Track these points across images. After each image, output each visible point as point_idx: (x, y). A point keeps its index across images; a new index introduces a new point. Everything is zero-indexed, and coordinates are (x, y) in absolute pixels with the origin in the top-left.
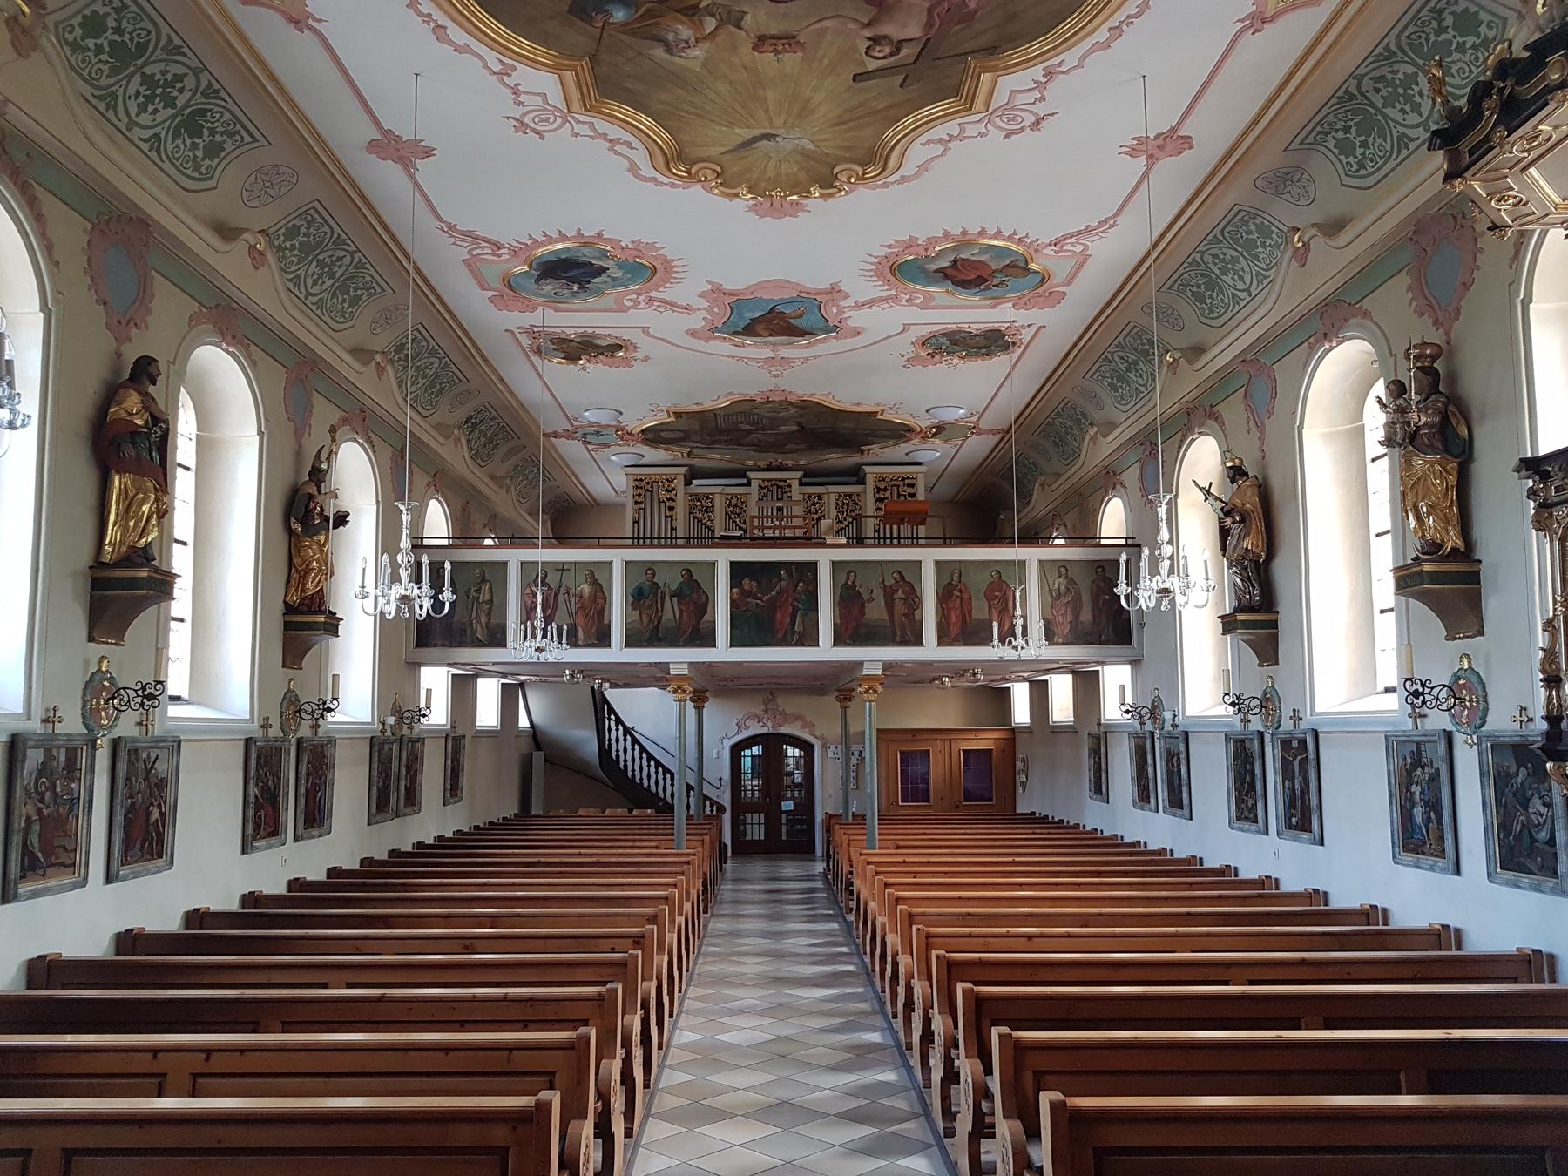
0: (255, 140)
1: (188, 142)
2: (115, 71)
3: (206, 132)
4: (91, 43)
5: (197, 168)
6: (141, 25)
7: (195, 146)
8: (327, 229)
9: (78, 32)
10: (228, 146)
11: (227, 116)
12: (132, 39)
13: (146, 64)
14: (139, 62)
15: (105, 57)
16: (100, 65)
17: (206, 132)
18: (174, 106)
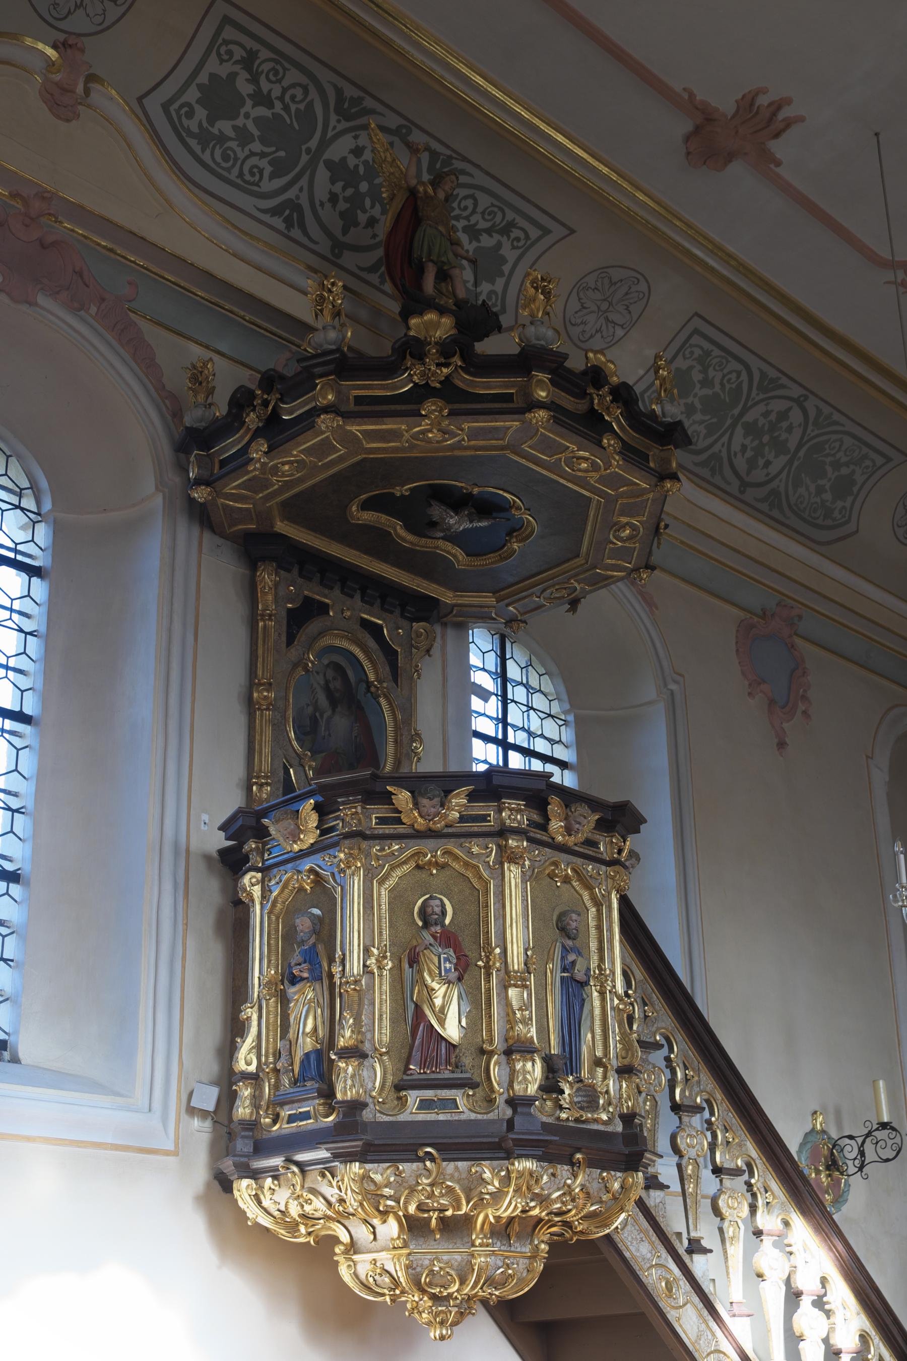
0: (546, 231)
2: (279, 169)
4: (225, 126)
8: (734, 365)
9: (201, 113)
10: (507, 251)
11: (484, 201)
12: (286, 108)
13: (324, 144)
14: (313, 144)
15: (257, 147)
16: (254, 160)
18: (329, 164)
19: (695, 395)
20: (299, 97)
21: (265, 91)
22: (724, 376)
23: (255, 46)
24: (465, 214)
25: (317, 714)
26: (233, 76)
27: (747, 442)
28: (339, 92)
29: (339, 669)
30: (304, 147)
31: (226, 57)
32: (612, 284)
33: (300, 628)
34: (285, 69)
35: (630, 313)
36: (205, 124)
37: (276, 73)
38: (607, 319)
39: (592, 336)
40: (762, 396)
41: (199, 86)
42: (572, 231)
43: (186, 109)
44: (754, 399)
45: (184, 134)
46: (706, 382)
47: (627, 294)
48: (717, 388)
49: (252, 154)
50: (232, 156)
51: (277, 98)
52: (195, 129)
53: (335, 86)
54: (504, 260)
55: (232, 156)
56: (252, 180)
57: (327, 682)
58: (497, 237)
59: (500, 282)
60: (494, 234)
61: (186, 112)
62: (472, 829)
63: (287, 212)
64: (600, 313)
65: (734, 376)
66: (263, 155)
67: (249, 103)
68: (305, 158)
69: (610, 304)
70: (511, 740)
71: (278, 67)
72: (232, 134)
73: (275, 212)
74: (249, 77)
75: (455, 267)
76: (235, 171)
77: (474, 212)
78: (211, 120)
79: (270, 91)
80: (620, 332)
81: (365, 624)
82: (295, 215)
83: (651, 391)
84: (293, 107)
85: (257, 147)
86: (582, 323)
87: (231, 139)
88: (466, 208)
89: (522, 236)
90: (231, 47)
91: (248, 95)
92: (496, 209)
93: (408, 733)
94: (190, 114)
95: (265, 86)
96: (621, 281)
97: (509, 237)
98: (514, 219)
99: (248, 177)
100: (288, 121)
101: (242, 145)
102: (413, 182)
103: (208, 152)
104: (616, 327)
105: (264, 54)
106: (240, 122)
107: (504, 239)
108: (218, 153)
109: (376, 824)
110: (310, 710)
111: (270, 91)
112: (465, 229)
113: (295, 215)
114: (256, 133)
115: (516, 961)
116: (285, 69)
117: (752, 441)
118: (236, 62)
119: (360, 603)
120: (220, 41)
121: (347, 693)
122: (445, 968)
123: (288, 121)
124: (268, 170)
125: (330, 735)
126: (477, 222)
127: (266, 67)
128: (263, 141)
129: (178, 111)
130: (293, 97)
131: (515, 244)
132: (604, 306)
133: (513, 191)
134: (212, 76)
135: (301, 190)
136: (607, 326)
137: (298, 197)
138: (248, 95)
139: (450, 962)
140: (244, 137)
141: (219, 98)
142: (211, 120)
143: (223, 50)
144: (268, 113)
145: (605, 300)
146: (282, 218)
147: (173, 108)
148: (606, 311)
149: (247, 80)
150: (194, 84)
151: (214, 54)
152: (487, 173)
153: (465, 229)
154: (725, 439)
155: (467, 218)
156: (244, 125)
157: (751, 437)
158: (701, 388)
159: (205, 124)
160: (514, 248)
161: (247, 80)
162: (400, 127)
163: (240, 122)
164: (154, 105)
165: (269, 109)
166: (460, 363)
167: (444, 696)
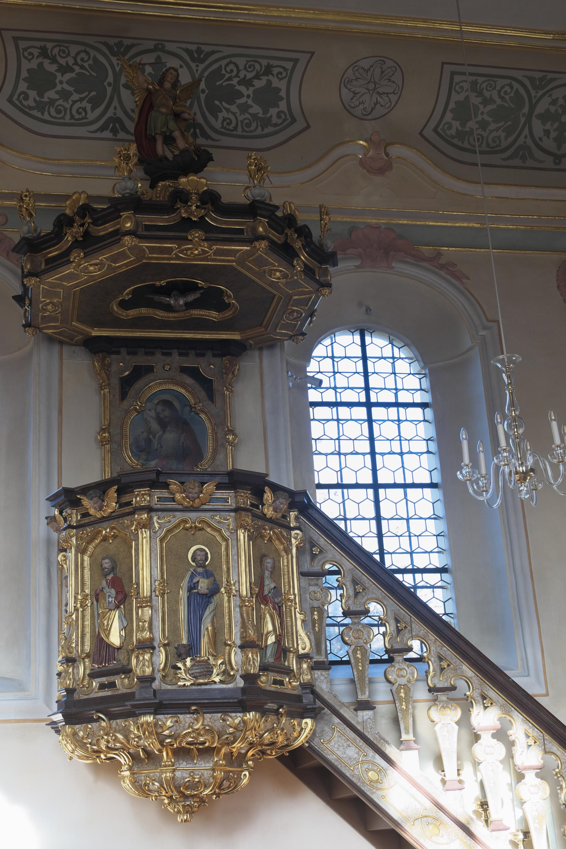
0: (296, 61)
1: (234, 108)
2: (95, 103)
3: (242, 89)
4: (51, 94)
5: (266, 122)
6: (73, 54)
7: (244, 108)
8: (501, 82)
9: (33, 94)
10: (276, 83)
11: (241, 62)
12: (82, 67)
14: (110, 79)
15: (75, 97)
16: (78, 105)
17: (242, 89)
19: (482, 113)
21: (64, 64)
22: (499, 92)
23: (42, 44)
24: (234, 74)
25: (151, 437)
26: (41, 65)
27: (548, 126)
28: (106, 44)
29: (167, 404)
30: (106, 84)
31: (30, 57)
33: (131, 386)
34: (67, 47)
35: (394, 82)
36: (38, 99)
37: (64, 52)
38: (378, 93)
39: (373, 109)
40: (541, 93)
41: (25, 80)
42: (313, 53)
43: (23, 95)
44: (535, 96)
45: (27, 110)
46: (486, 102)
47: (382, 72)
48: (499, 101)
49: (74, 102)
50: (62, 109)
51: (73, 64)
52: (32, 104)
53: (101, 43)
54: (279, 90)
55: (62, 109)
56: (81, 116)
57: (158, 414)
58: (264, 78)
59: (283, 105)
60: (261, 77)
61: (23, 98)
62: (125, 511)
63: (111, 125)
64: (371, 92)
65: (507, 88)
66: (81, 100)
67: (59, 75)
68: (109, 90)
69: (375, 83)
70: (373, 399)
71: (62, 48)
72: (57, 97)
73: (102, 129)
74: (49, 61)
75: (173, 131)
76: (68, 116)
77: (239, 71)
78: (41, 95)
79: (67, 63)
80: (394, 98)
81: (184, 370)
82: (117, 125)
83: (442, 124)
84: (86, 65)
85: (75, 97)
86: (360, 104)
87: (57, 100)
88: (232, 71)
89: (281, 70)
90: (29, 51)
91: (56, 71)
92: (252, 63)
93: (225, 429)
94: (26, 97)
95: (63, 62)
96: (372, 66)
98: (268, 63)
99: (77, 116)
100: (88, 74)
101: (66, 100)
102: (145, 85)
103: (46, 113)
104: (389, 95)
105: (49, 45)
106: (59, 87)
107: (270, 77)
108: (53, 111)
109: (81, 518)
110: (145, 434)
111: (67, 63)
112: (239, 83)
113: (117, 125)
114: (71, 89)
115: (146, 589)
117: (552, 125)
118: (38, 57)
119: (178, 358)
120: (21, 51)
121: (176, 417)
122: (109, 601)
123: (88, 74)
124: (89, 107)
125: (161, 447)
126: (245, 75)
127: (56, 51)
128: (77, 91)
129: (18, 99)
130: (82, 59)
131: (280, 76)
132: (371, 86)
133: (253, 48)
134: (29, 71)
135: (115, 108)
136: (381, 98)
137: (115, 114)
138: (56, 71)
139: (112, 598)
140: (65, 95)
141: (40, 81)
142: (41, 95)
143: (26, 54)
144: (73, 75)
145: (369, 82)
146: (109, 131)
147: (14, 99)
148: (375, 89)
149: (50, 63)
150: (21, 79)
151: (23, 60)
152: (229, 46)
153: (239, 83)
154: (526, 131)
155: (237, 76)
156: (62, 88)
157: (550, 122)
158: (484, 107)
159: (38, 99)
160: (280, 79)
161: (50, 63)
162: (155, 46)
163: (59, 87)
165: (73, 72)
166: (89, 221)
167: (263, 396)
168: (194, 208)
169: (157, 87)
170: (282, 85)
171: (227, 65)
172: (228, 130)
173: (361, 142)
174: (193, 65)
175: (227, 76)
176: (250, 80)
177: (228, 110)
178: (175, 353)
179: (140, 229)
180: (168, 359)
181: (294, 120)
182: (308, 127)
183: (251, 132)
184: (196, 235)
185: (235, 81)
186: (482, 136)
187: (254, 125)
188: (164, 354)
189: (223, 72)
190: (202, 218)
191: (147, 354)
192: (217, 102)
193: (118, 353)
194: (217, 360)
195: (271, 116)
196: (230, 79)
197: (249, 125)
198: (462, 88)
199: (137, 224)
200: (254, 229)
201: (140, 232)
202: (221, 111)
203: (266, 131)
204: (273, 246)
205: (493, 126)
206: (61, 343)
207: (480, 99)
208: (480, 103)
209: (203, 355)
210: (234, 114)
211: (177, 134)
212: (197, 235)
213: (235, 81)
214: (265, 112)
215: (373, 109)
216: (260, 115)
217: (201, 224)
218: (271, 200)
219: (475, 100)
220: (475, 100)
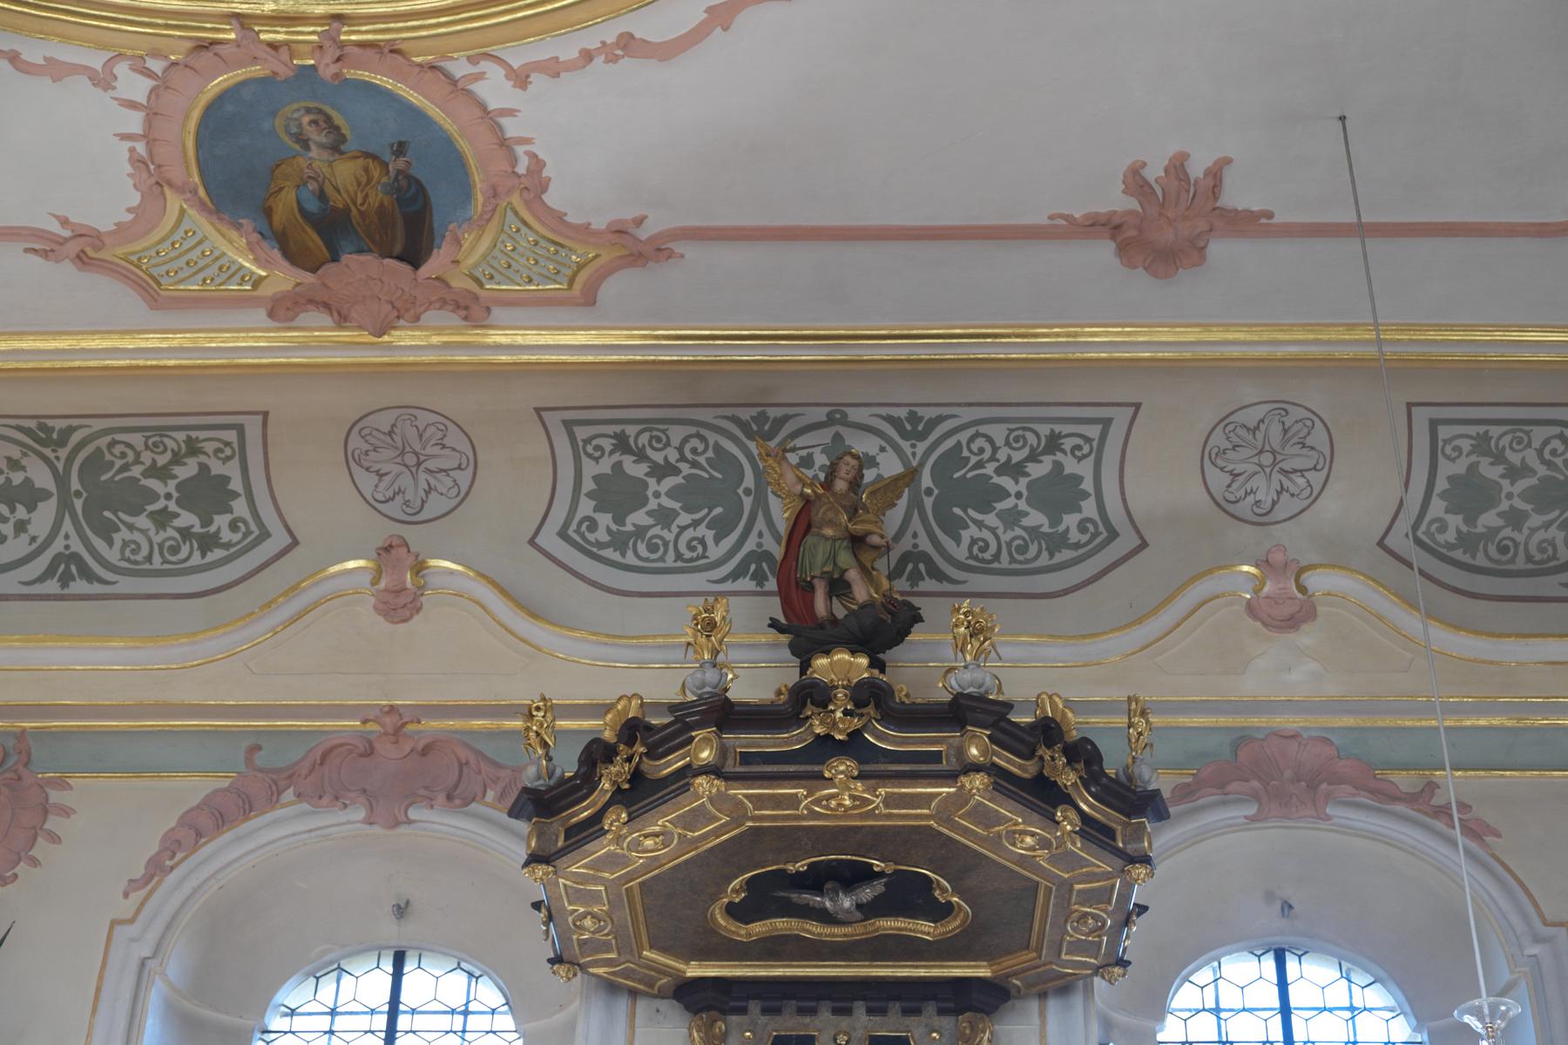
2: (722, 528)
4: (639, 518)
5: (1058, 541)
6: (676, 442)
8: (1539, 434)
9: (605, 520)
10: (1071, 466)
11: (998, 433)
12: (694, 464)
16: (689, 533)
17: (1006, 482)
20: (701, 448)
22: (1540, 452)
23: (618, 428)
26: (618, 466)
28: (735, 420)
30: (740, 491)
31: (598, 454)
32: (1254, 431)
34: (663, 431)
36: (614, 527)
37: (659, 440)
38: (1284, 472)
39: (1274, 503)
41: (590, 495)
42: (1138, 406)
46: (1514, 473)
47: (1285, 431)
48: (1542, 471)
49: (683, 529)
52: (605, 538)
54: (1078, 479)
59: (1089, 508)
63: (753, 567)
64: (1268, 470)
66: (695, 524)
67: (652, 481)
68: (748, 502)
69: (1273, 452)
72: (651, 521)
73: (735, 575)
76: (671, 554)
77: (995, 449)
78: (619, 520)
79: (666, 458)
84: (702, 460)
85: (684, 519)
88: (982, 450)
90: (595, 442)
92: (1020, 432)
94: (593, 526)
95: (658, 457)
97: (1064, 452)
99: (688, 555)
101: (667, 526)
103: (630, 553)
105: (631, 430)
106: (653, 504)
107: (1059, 456)
111: (666, 458)
116: (663, 431)
118: (611, 453)
124: (709, 535)
127: (644, 439)
128: (688, 509)
129: (577, 531)
130: (694, 451)
131: (1078, 453)
132: (1267, 459)
133: (1018, 405)
134: (596, 478)
135: (760, 535)
136: (1291, 480)
140: (664, 517)
141: (617, 495)
142: (619, 520)
143: (590, 449)
144: (679, 480)
145: (1261, 452)
148: (1274, 464)
151: (584, 458)
153: (999, 471)
155: (993, 458)
159: (614, 527)
160: (1080, 459)
163: (653, 504)
164: (549, 539)
168: (839, 714)
169: (820, 491)
170: (1085, 469)
171: (971, 439)
172: (983, 561)
173: (1246, 568)
174: (905, 445)
175: (974, 460)
176: (1021, 464)
177: (980, 525)
178: (860, 1008)
179: (730, 762)
180: (844, 1022)
181: (1113, 535)
182: (1144, 545)
183: (1027, 561)
184: (841, 768)
185: (990, 469)
186: (1513, 540)
187: (1033, 549)
188: (837, 1011)
189: (965, 453)
190: (856, 735)
191: (802, 1011)
192: (957, 511)
193: (743, 1011)
194: (947, 1022)
195: (1068, 529)
196: (980, 465)
197: (1023, 549)
198: (1458, 449)
199: (723, 752)
200: (961, 752)
201: (731, 766)
202: (966, 527)
203: (1060, 557)
204: (1003, 781)
205: (1536, 520)
206: (634, 994)
207: (1500, 469)
208: (1503, 476)
209: (917, 1012)
210: (993, 531)
211: (853, 575)
212: (842, 768)
213: (990, 469)
214: (1055, 522)
215: (1274, 503)
216: (1046, 529)
217: (854, 746)
218: (1000, 691)
219: (1491, 472)
220: (1491, 472)
